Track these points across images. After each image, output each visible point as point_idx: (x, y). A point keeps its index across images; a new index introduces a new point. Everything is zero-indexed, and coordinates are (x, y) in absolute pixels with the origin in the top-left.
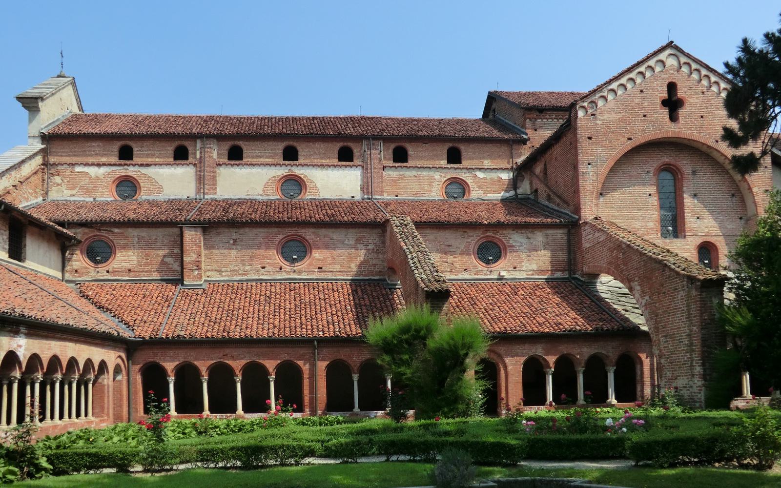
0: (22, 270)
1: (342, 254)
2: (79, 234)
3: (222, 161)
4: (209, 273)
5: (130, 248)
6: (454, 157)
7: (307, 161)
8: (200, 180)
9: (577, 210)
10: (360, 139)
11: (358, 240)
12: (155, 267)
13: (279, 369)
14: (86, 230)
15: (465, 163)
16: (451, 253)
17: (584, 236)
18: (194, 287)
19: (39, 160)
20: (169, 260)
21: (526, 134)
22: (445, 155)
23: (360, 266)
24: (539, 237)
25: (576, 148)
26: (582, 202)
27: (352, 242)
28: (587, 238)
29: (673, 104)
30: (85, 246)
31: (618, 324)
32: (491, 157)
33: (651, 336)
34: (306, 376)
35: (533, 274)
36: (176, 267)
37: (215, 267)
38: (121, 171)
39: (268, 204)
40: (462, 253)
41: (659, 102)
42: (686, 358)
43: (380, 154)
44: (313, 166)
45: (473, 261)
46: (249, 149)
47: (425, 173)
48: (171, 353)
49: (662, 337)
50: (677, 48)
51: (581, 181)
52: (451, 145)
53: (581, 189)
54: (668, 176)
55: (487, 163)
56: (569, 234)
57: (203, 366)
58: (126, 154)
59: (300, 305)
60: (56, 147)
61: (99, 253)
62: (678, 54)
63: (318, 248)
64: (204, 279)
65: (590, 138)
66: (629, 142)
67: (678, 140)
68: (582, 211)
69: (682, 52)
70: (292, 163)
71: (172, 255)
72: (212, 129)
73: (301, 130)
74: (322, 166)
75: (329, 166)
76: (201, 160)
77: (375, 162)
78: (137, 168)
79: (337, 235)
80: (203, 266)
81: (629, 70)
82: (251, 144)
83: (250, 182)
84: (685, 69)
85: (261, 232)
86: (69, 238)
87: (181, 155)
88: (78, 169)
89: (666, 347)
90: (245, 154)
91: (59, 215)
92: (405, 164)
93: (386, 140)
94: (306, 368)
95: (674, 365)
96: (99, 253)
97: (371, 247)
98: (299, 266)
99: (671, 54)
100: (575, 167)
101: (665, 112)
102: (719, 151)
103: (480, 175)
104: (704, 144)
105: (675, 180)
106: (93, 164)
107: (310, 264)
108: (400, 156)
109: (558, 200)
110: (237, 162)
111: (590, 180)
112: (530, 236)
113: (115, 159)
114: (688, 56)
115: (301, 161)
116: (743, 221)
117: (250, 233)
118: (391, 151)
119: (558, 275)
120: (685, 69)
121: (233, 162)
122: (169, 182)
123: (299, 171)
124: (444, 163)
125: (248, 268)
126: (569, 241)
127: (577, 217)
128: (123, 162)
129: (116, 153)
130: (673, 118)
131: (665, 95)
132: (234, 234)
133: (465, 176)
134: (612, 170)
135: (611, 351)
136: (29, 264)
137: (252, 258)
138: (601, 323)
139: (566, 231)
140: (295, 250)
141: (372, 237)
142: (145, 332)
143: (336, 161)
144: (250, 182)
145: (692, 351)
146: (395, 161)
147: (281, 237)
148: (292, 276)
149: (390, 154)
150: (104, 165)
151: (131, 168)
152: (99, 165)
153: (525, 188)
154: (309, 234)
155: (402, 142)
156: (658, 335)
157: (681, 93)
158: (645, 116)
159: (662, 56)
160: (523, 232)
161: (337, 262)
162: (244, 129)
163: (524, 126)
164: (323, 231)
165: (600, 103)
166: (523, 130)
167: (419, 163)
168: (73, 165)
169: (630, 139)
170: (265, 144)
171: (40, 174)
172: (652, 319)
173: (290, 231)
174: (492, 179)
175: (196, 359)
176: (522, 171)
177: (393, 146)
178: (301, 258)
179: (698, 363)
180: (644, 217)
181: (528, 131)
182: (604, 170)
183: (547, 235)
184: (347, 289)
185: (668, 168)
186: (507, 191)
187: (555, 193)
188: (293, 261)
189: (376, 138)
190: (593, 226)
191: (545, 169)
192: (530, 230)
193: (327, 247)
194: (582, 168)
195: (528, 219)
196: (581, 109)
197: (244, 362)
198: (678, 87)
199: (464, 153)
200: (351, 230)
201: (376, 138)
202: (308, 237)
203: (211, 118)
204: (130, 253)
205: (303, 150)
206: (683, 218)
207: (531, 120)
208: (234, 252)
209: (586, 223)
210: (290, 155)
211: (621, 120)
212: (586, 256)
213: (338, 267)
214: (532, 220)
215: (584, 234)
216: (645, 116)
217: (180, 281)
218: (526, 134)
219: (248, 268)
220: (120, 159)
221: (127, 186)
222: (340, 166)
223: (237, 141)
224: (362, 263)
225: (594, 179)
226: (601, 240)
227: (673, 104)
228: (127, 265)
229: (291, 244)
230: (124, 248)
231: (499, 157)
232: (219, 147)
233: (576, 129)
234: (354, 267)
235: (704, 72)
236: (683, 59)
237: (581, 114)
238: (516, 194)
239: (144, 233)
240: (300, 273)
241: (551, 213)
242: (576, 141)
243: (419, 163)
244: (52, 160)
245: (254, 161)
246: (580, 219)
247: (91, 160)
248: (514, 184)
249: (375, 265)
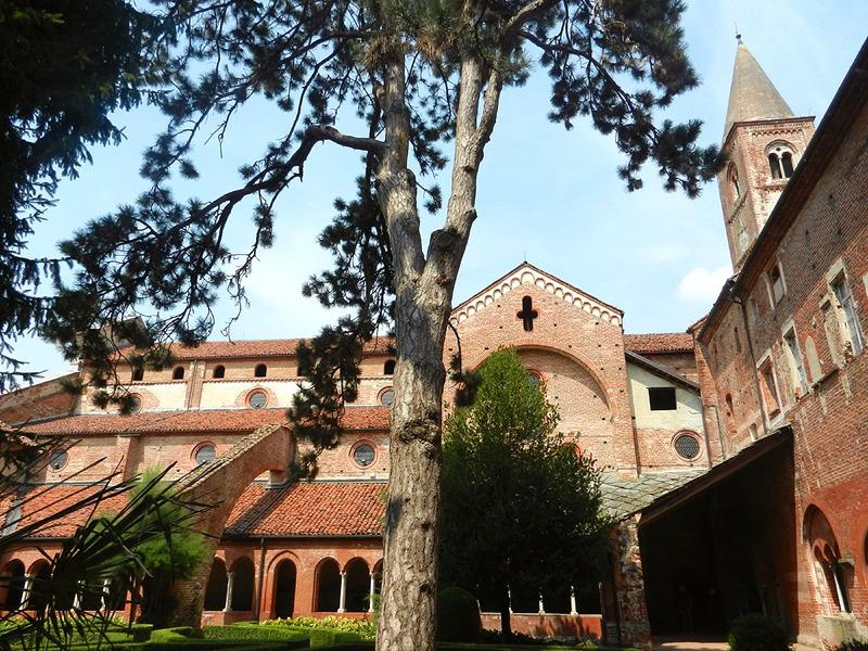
29: (528, 314)
50: (530, 266)
62: (533, 272)
69: (537, 270)
81: (487, 289)
114: (542, 272)
123: (264, 385)
130: (528, 327)
131: (521, 308)
154: (215, 439)
159: (518, 275)
173: (203, 438)
211: (480, 332)
227: (528, 314)
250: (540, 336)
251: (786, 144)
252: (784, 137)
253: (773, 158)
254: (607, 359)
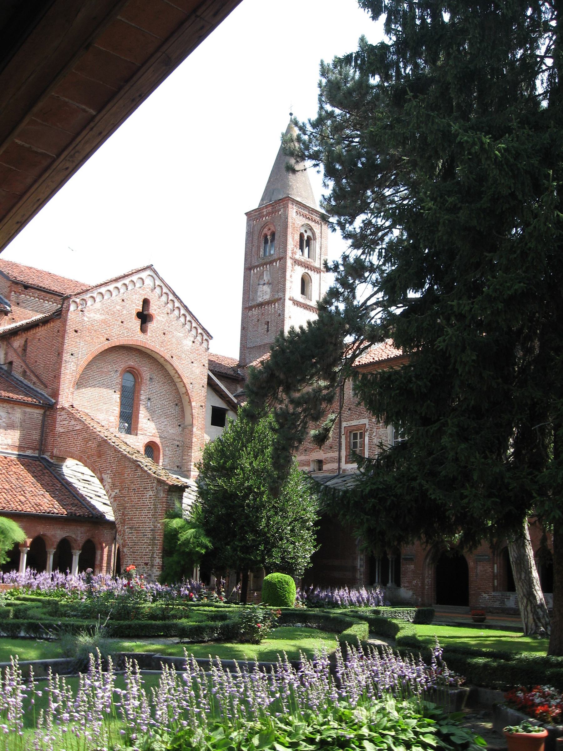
9: (55, 394)
17: (58, 420)
24: (18, 414)
25: (63, 337)
26: (62, 387)
28: (62, 423)
29: (144, 317)
31: (88, 511)
33: (117, 526)
35: (7, 449)
41: (135, 313)
42: (147, 549)
49: (127, 528)
51: (63, 368)
53: (62, 376)
54: (130, 377)
56: (44, 415)
65: (76, 331)
66: (107, 342)
67: (143, 349)
68: (60, 396)
84: (158, 290)
89: (130, 538)
95: (137, 555)
99: (149, 275)
100: (60, 354)
101: (139, 322)
102: (172, 366)
104: (162, 357)
105: (135, 382)
109: (35, 379)
111: (71, 369)
112: (10, 411)
114: (162, 280)
116: (181, 429)
119: (29, 453)
120: (158, 290)
126: (43, 421)
127: (54, 401)
130: (143, 330)
131: (140, 309)
134: (88, 364)
135: (79, 535)
138: (74, 508)
139: (42, 411)
145: (154, 544)
156: (124, 526)
157: (153, 309)
158: (122, 322)
159: (144, 275)
160: (5, 406)
163: (8, 297)
165: (90, 302)
166: (6, 301)
169: (107, 339)
172: (120, 511)
179: (158, 555)
180: (107, 412)
182: (83, 363)
183: (25, 413)
185: (131, 371)
187: (32, 372)
190: (69, 413)
192: (11, 405)
194: (66, 356)
195: (11, 395)
196: (73, 303)
198: (151, 304)
206: (137, 417)
207: (15, 293)
209: (63, 409)
211: (104, 321)
212: (59, 439)
214: (15, 396)
215: (59, 418)
216: (122, 322)
218: (10, 307)
225: (74, 369)
226: (77, 428)
227: (144, 317)
233: (66, 321)
235: (171, 297)
236: (158, 282)
237: (72, 307)
241: (28, 391)
242: (65, 331)
246: (56, 403)
250: (151, 340)
251: (311, 229)
252: (312, 224)
253: (301, 235)
254: (195, 377)
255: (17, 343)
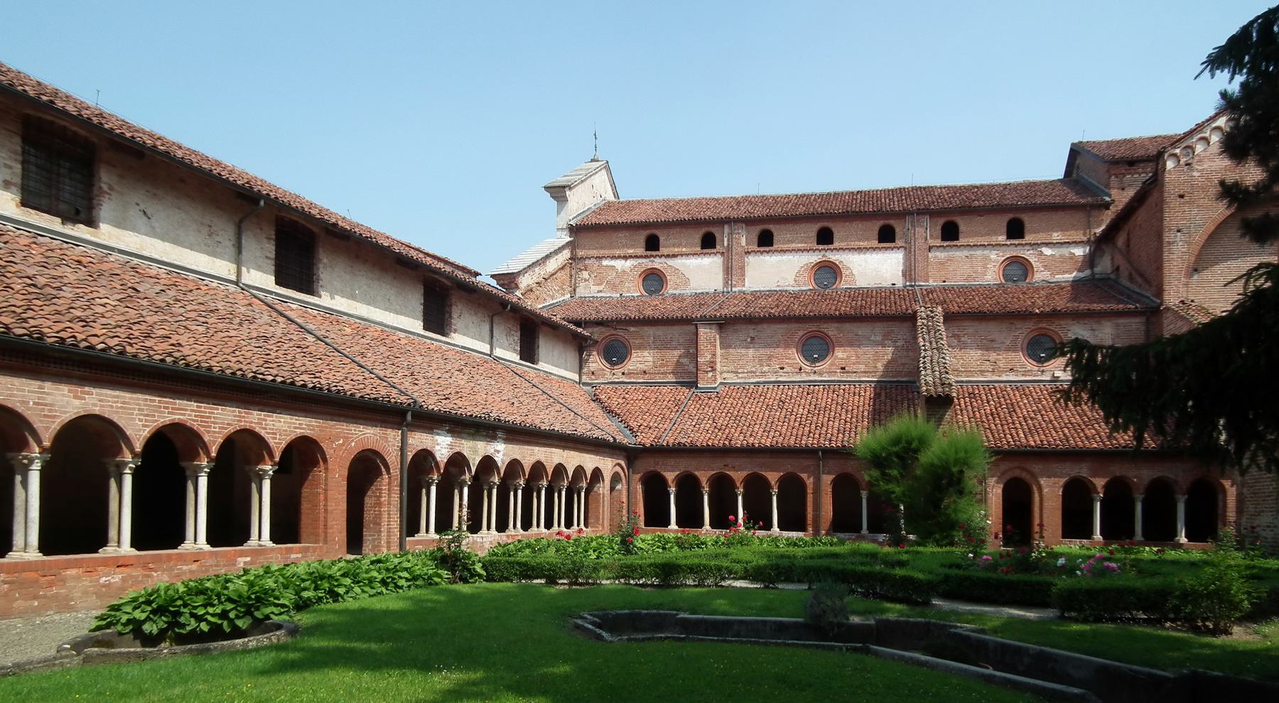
0: (532, 373)
1: (868, 352)
2: (596, 333)
3: (751, 248)
4: (725, 375)
5: (645, 349)
6: (1015, 231)
7: (843, 245)
8: (728, 270)
10: (902, 215)
11: (886, 336)
12: (670, 369)
13: (782, 482)
14: (603, 329)
15: (1029, 238)
16: (994, 349)
18: (707, 391)
19: (566, 254)
20: (684, 361)
21: (1110, 196)
22: (1005, 230)
23: (886, 366)
27: (879, 338)
30: (601, 347)
32: (1063, 229)
34: (810, 491)
36: (692, 368)
37: (731, 368)
38: (647, 264)
39: (796, 296)
40: (1008, 349)
43: (926, 232)
44: (850, 250)
45: (1021, 359)
46: (779, 233)
47: (979, 252)
48: (672, 462)
52: (1011, 216)
55: (1056, 236)
57: (704, 477)
58: (652, 244)
59: (816, 410)
60: (585, 238)
61: (616, 354)
63: (842, 346)
64: (719, 381)
70: (826, 247)
71: (687, 355)
72: (742, 212)
73: (837, 207)
74: (859, 250)
75: (867, 249)
76: (729, 248)
77: (920, 242)
78: (663, 259)
79: (862, 330)
80: (718, 367)
82: (783, 227)
83: (779, 272)
85: (780, 328)
86: (585, 338)
87: (708, 243)
88: (605, 262)
90: (775, 239)
91: (579, 314)
92: (955, 243)
93: (933, 214)
94: (810, 482)
96: (616, 354)
97: (900, 344)
98: (821, 366)
103: (1047, 251)
106: (619, 257)
107: (832, 365)
108: (950, 233)
110: (767, 249)
113: (641, 251)
115: (836, 244)
117: (768, 329)
118: (939, 228)
121: (762, 249)
122: (697, 274)
124: (1002, 238)
125: (766, 369)
128: (649, 253)
129: (643, 244)
132: (751, 331)
133: (1029, 254)
136: (542, 365)
137: (770, 358)
140: (816, 348)
141: (901, 331)
142: (647, 439)
143: (875, 243)
144: (779, 272)
146: (944, 239)
147: (801, 333)
148: (812, 378)
149: (938, 231)
150: (631, 257)
151: (657, 260)
152: (625, 258)
153: (1104, 266)
154: (831, 330)
155: (950, 214)
161: (861, 362)
162: (777, 210)
164: (847, 326)
167: (972, 241)
168: (600, 258)
170: (797, 227)
171: (567, 270)
173: (812, 327)
174: (1061, 256)
175: (698, 470)
176: (1101, 244)
177: (941, 221)
178: (822, 358)
181: (1114, 192)
184: (870, 393)
186: (1079, 270)
188: (814, 361)
189: (921, 212)
191: (1128, 240)
193: (851, 344)
197: (745, 473)
199: (1027, 226)
200: (878, 324)
201: (921, 212)
202: (830, 333)
203: (746, 199)
204: (646, 353)
205: (838, 231)
208: (751, 351)
210: (825, 238)
213: (862, 367)
217: (693, 384)
219: (766, 369)
220: (647, 250)
221: (654, 280)
222: (880, 249)
223: (766, 225)
224: (889, 362)
228: (643, 367)
229: (813, 341)
230: (639, 348)
231: (1074, 227)
232: (748, 232)
234: (880, 366)
238: (1093, 274)
239: (659, 331)
240: (821, 374)
243: (972, 241)
244: (580, 253)
245: (785, 247)
247: (617, 252)
248: (1090, 261)
249: (904, 364)
255: (1121, 241)
